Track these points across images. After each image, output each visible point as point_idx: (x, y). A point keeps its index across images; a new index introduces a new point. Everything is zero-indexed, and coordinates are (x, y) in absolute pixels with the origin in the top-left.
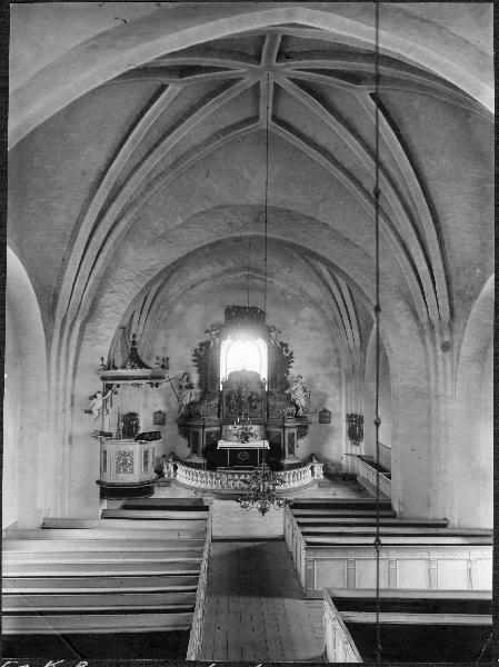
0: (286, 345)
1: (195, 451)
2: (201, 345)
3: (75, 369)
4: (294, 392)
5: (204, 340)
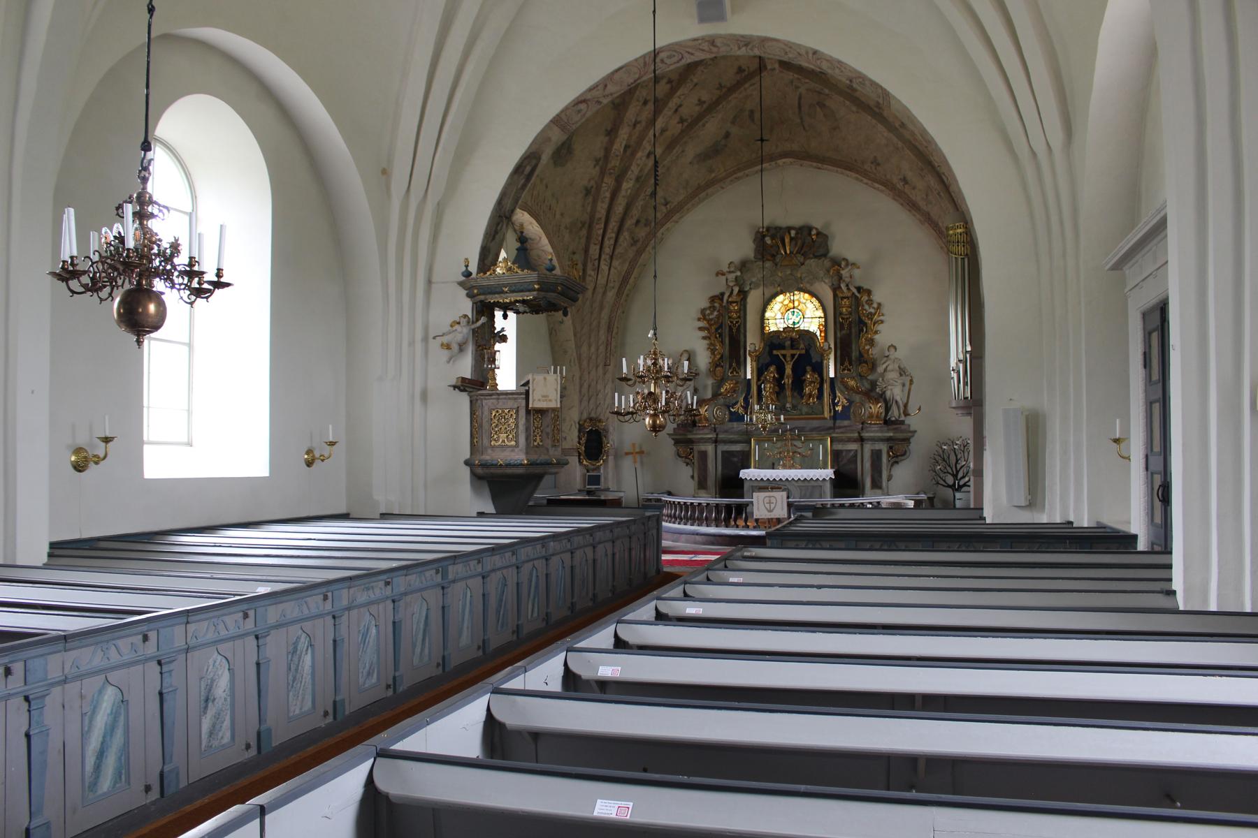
0: (869, 292)
1: (702, 485)
2: (713, 299)
3: (429, 282)
4: (882, 375)
5: (716, 292)
